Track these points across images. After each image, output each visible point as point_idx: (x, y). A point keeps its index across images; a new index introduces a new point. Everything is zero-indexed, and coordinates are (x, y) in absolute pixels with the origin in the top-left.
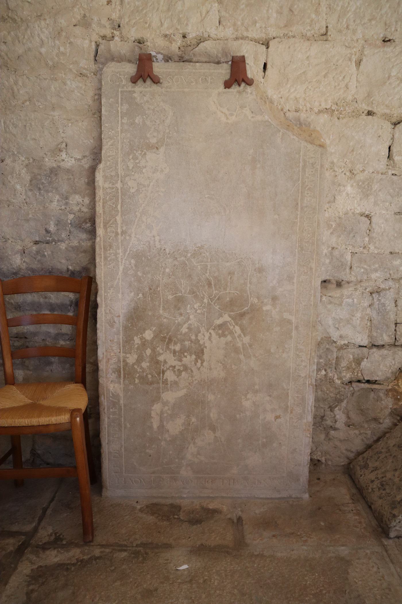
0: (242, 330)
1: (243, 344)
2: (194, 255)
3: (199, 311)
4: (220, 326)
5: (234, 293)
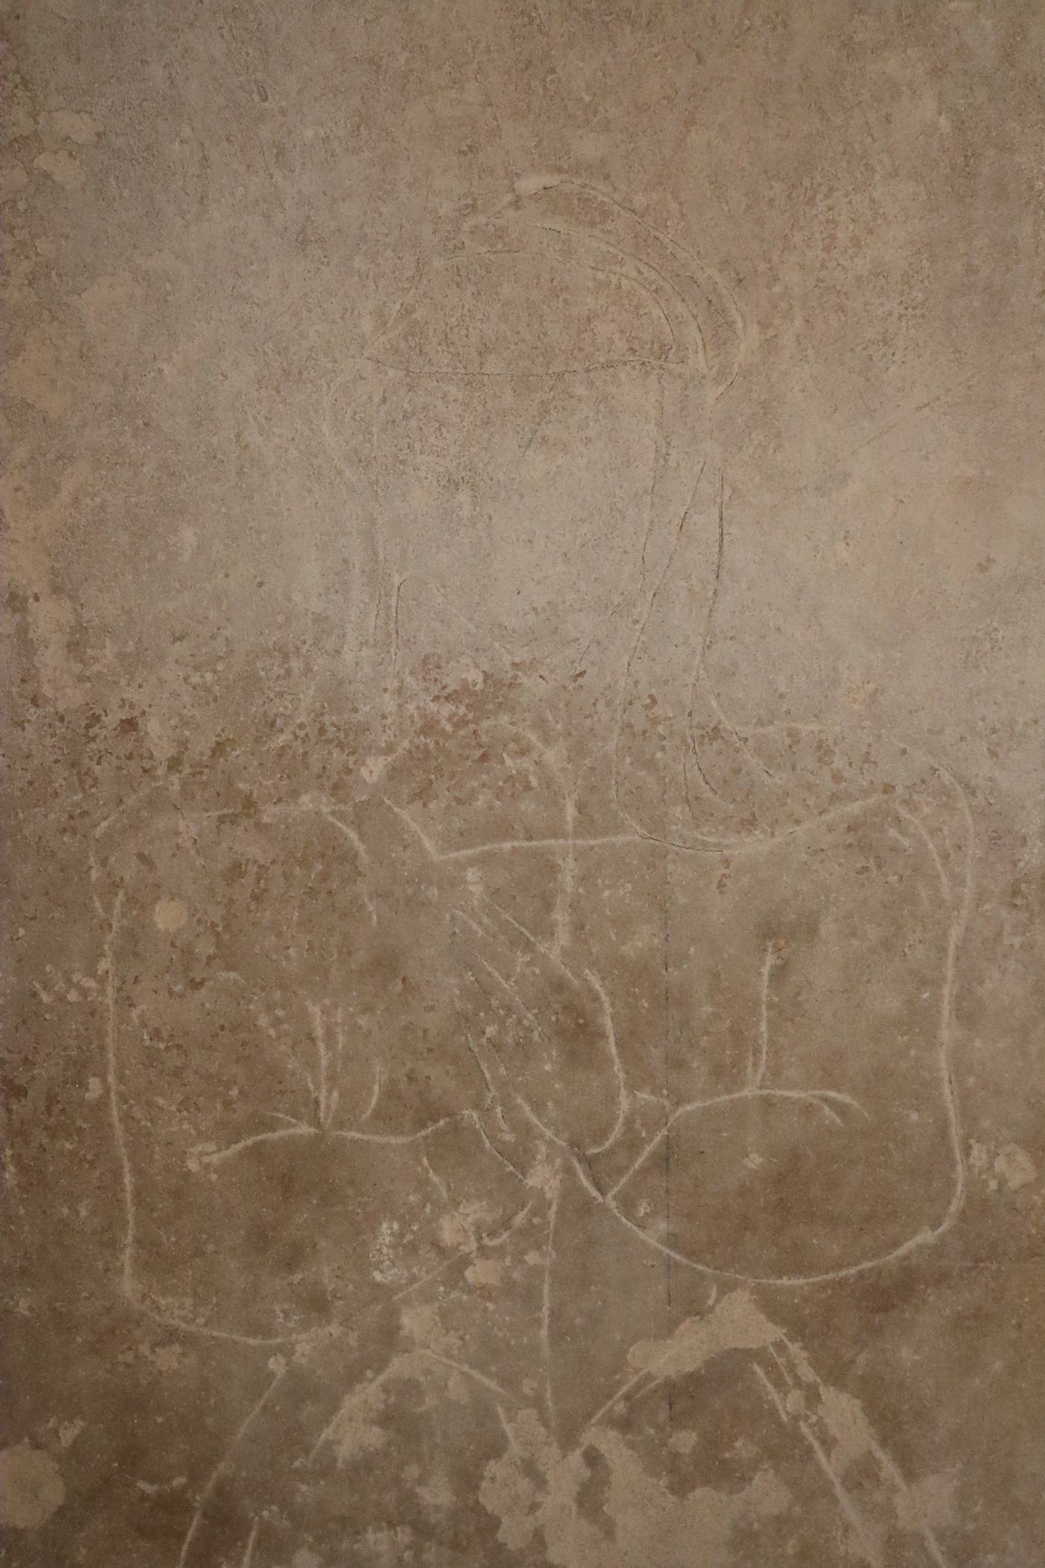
0: (886, 1421)
1: (895, 1543)
2: (420, 771)
3: (479, 1273)
4: (684, 1396)
5: (808, 1110)
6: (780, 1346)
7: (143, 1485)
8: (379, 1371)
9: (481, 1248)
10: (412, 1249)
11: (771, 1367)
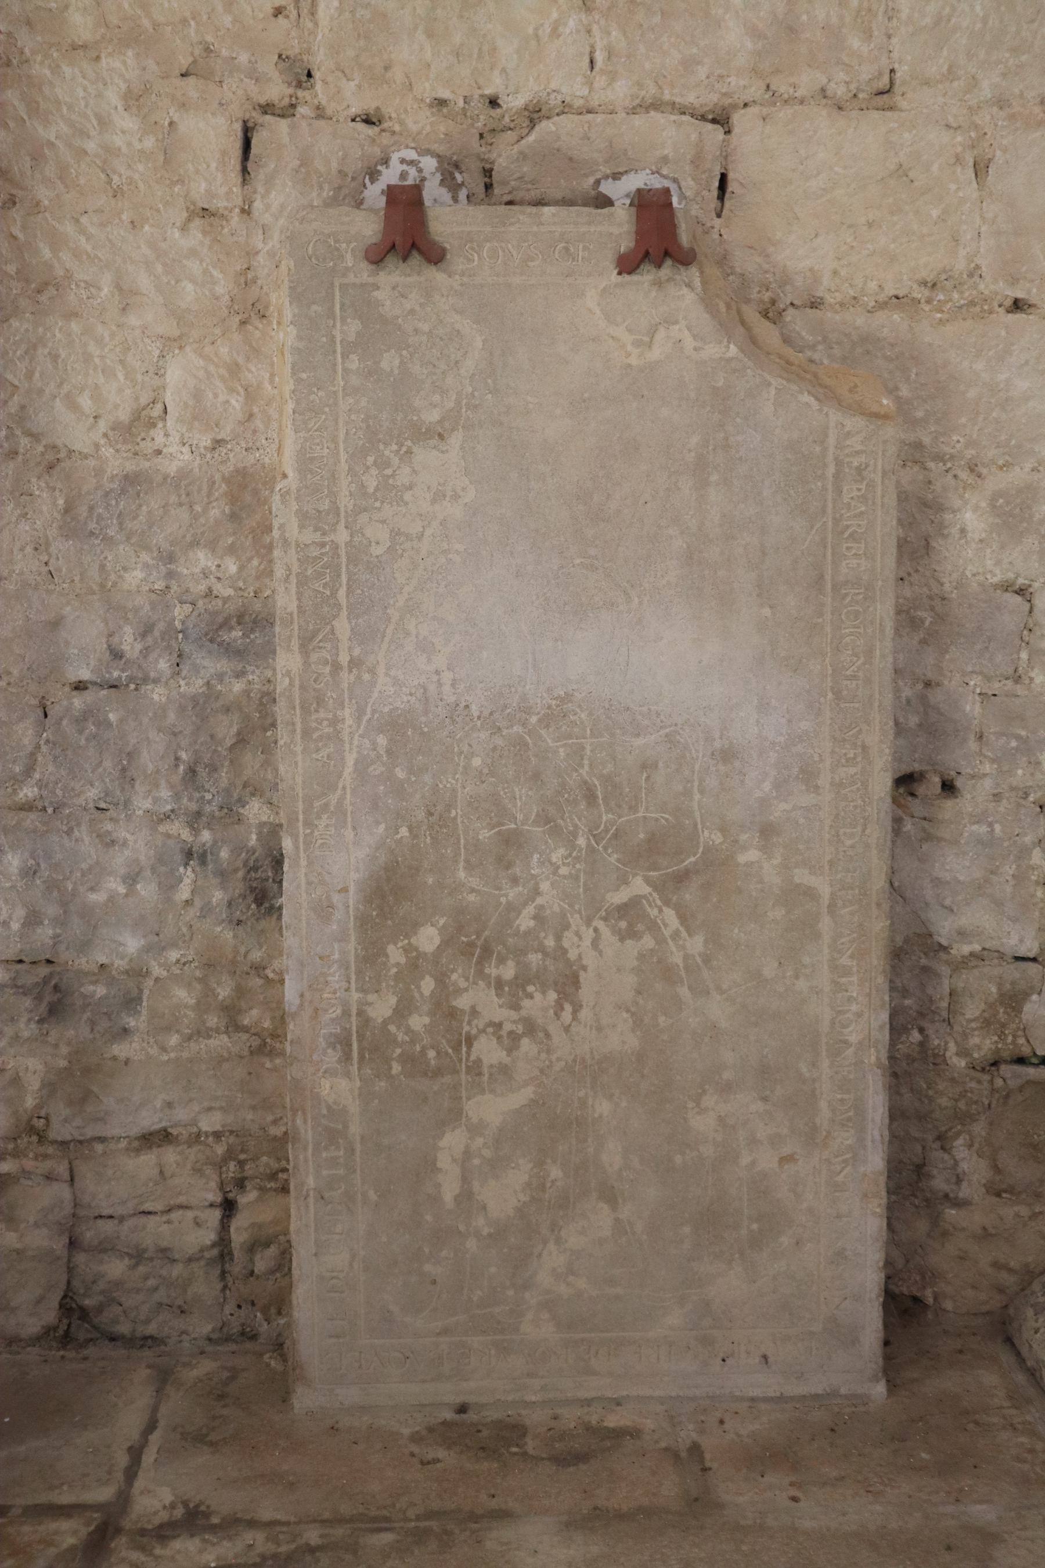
0: (683, 918)
1: (686, 957)
2: (546, 720)
3: (564, 871)
4: (623, 910)
5: (657, 820)
6: (650, 894)
7: (463, 938)
8: (533, 902)
9: (563, 863)
10: (543, 863)
11: (648, 901)
